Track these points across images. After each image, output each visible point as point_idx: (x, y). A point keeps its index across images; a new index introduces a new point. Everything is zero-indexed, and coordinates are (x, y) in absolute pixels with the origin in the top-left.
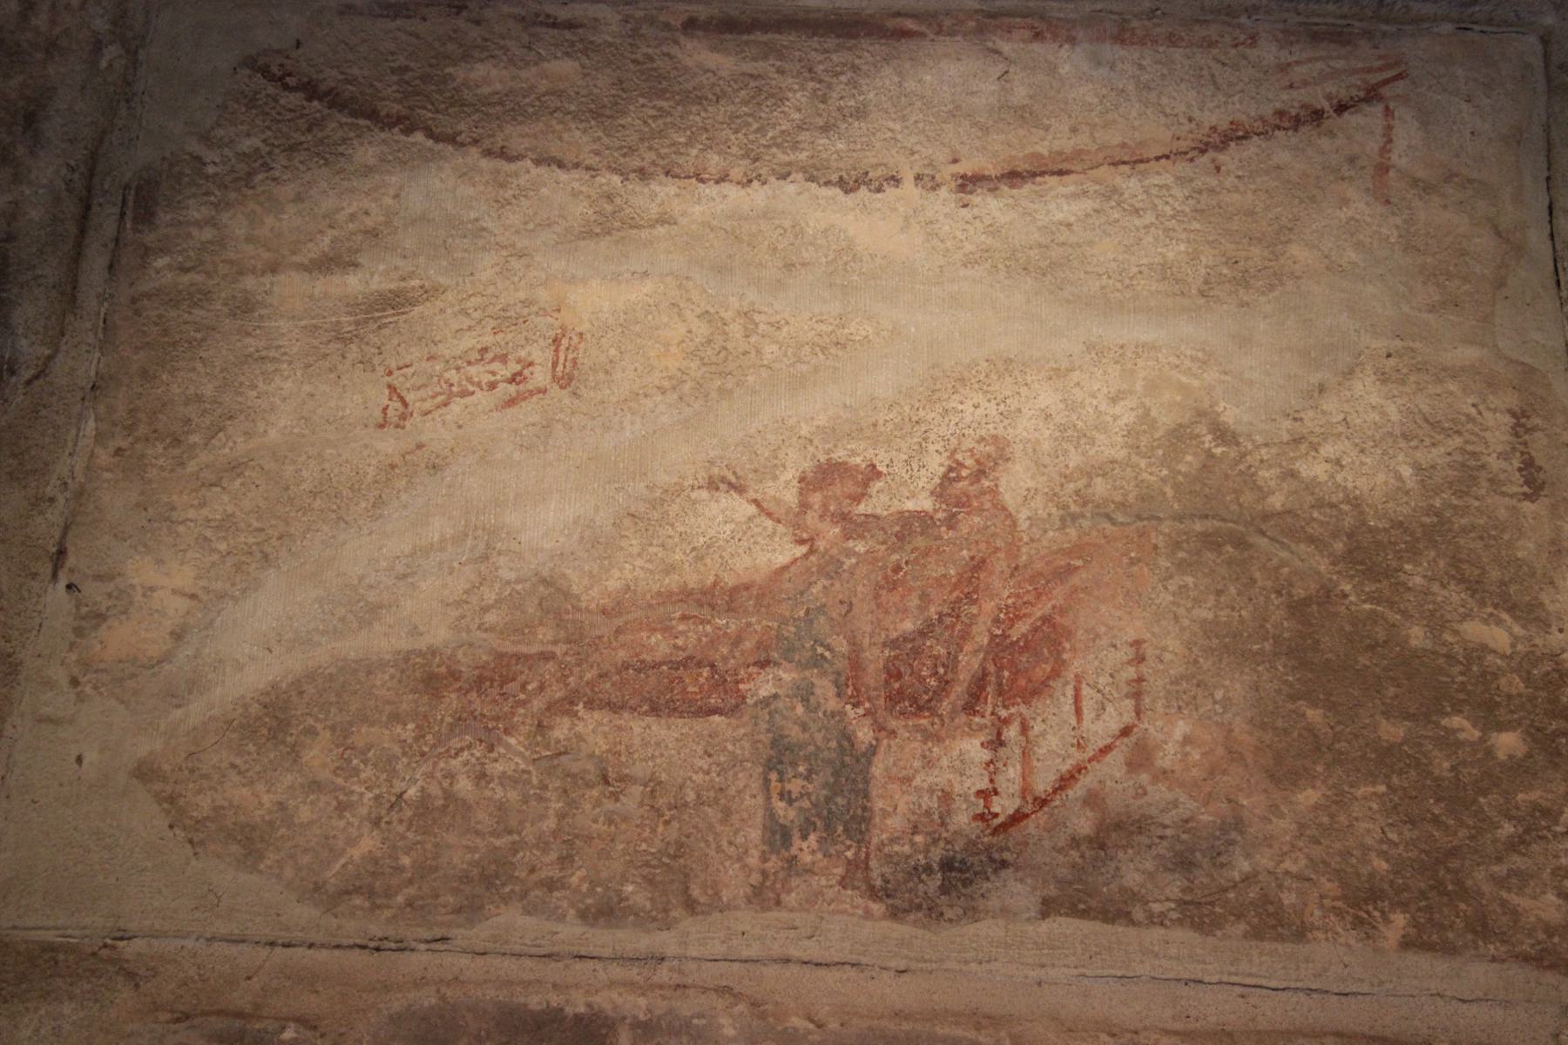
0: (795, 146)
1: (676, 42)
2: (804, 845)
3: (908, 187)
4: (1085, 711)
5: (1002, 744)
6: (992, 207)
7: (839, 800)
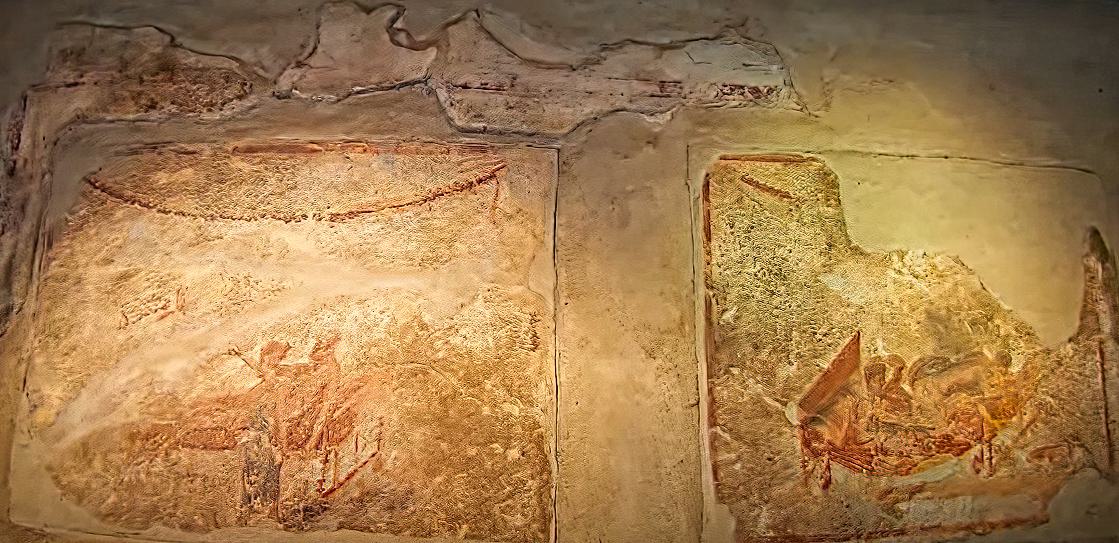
6: (342, 228)
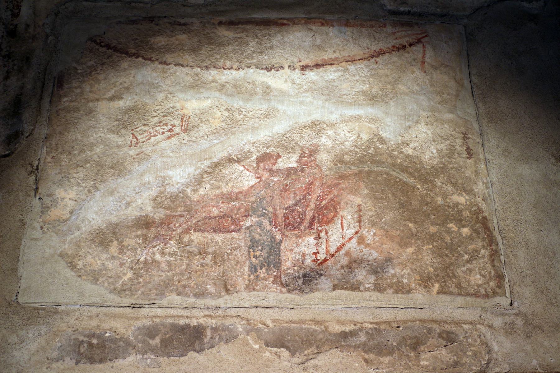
0: (252, 58)
1: (216, 28)
2: (261, 271)
3: (287, 70)
5: (320, 238)
7: (272, 257)
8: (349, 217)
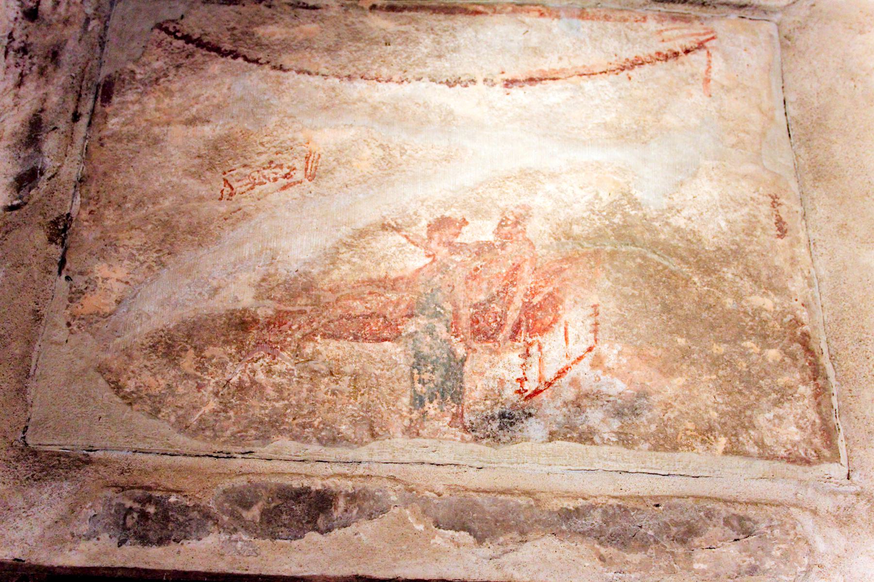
4: (570, 339)
8: (579, 324)
